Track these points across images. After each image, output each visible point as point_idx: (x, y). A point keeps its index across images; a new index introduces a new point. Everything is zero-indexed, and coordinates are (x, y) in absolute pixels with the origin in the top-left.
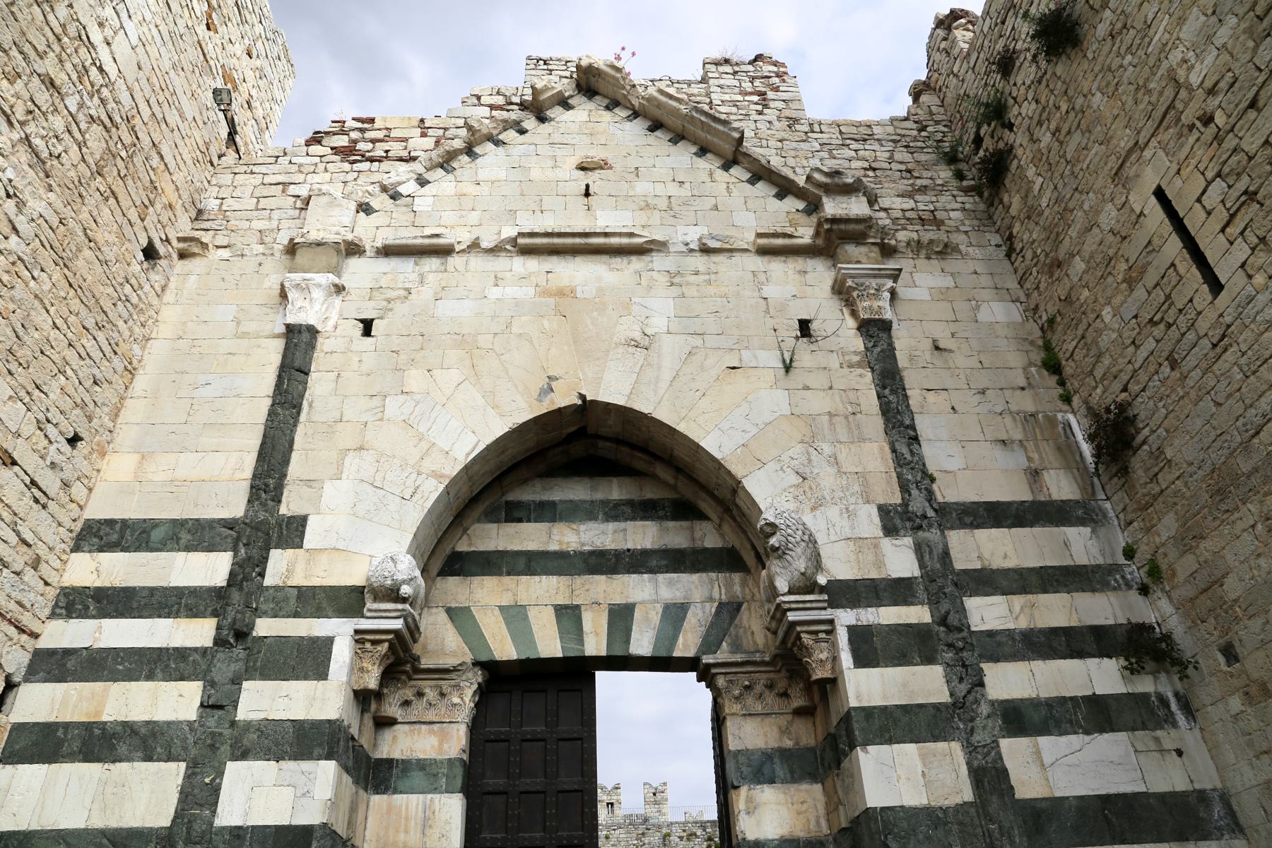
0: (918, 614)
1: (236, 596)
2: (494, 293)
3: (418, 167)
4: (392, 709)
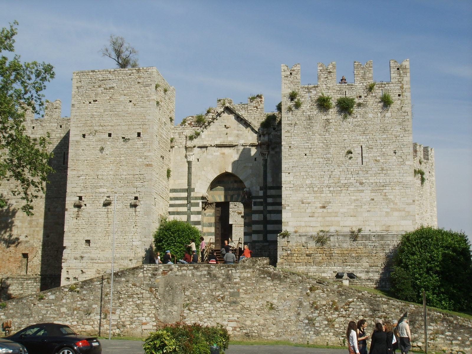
0: (262, 200)
1: (189, 198)
2: (214, 154)
3: (202, 129)
4: (206, 208)
